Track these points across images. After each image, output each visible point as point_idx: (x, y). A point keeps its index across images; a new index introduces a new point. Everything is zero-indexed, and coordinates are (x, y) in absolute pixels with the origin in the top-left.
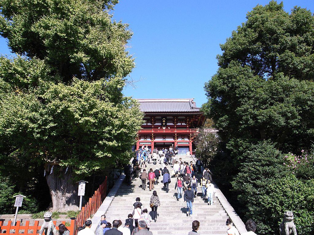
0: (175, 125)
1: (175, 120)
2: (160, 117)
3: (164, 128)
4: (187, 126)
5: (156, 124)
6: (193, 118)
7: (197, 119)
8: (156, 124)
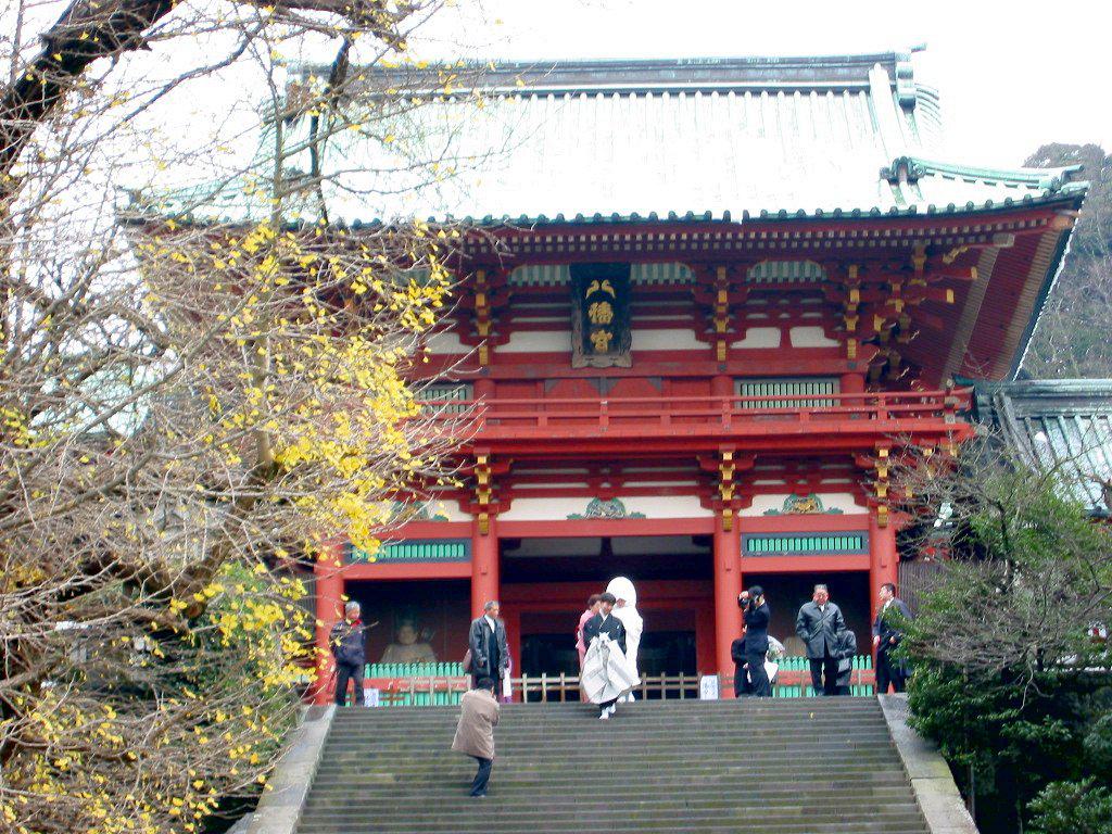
1: (723, 297)
2: (556, 274)
6: (908, 270)
7: (944, 286)
8: (522, 343)
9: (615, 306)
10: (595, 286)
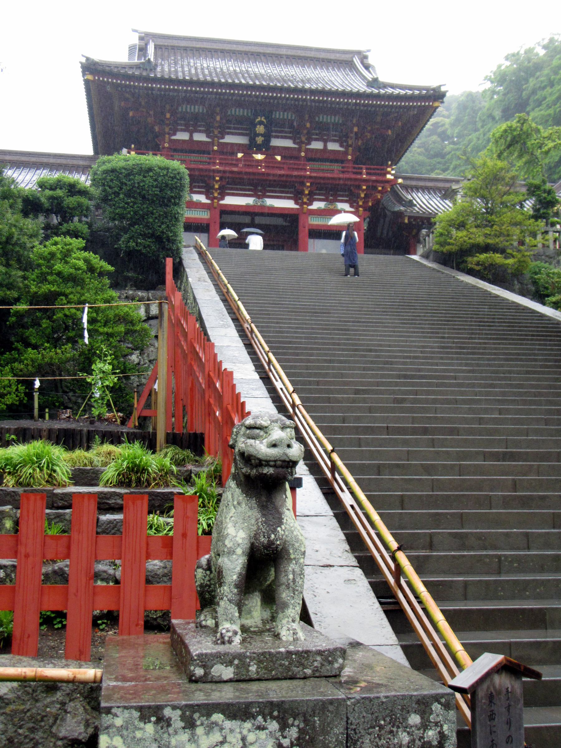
0: (303, 148)
3: (259, 157)
4: (346, 153)
5: (229, 139)
8: (229, 139)
9: (266, 126)
10: (259, 119)
